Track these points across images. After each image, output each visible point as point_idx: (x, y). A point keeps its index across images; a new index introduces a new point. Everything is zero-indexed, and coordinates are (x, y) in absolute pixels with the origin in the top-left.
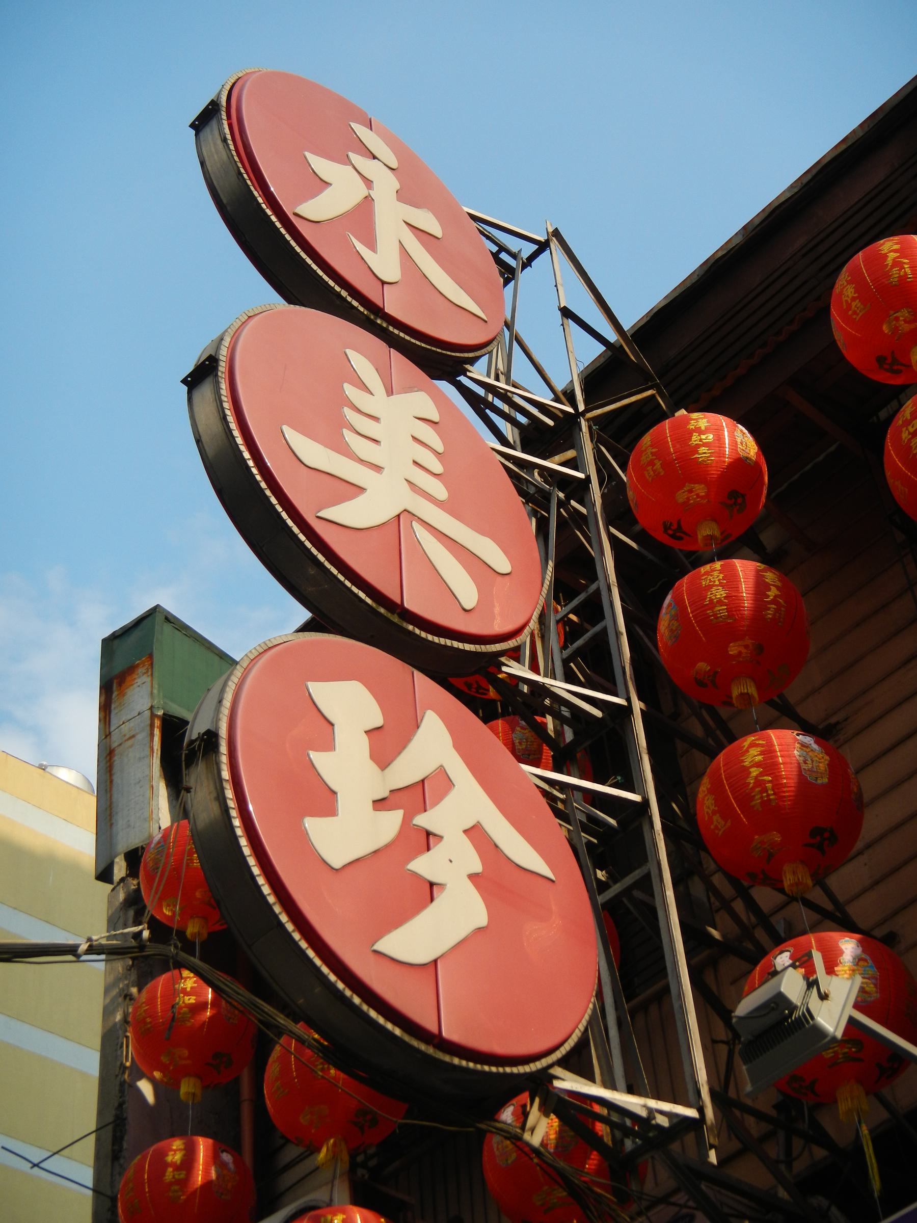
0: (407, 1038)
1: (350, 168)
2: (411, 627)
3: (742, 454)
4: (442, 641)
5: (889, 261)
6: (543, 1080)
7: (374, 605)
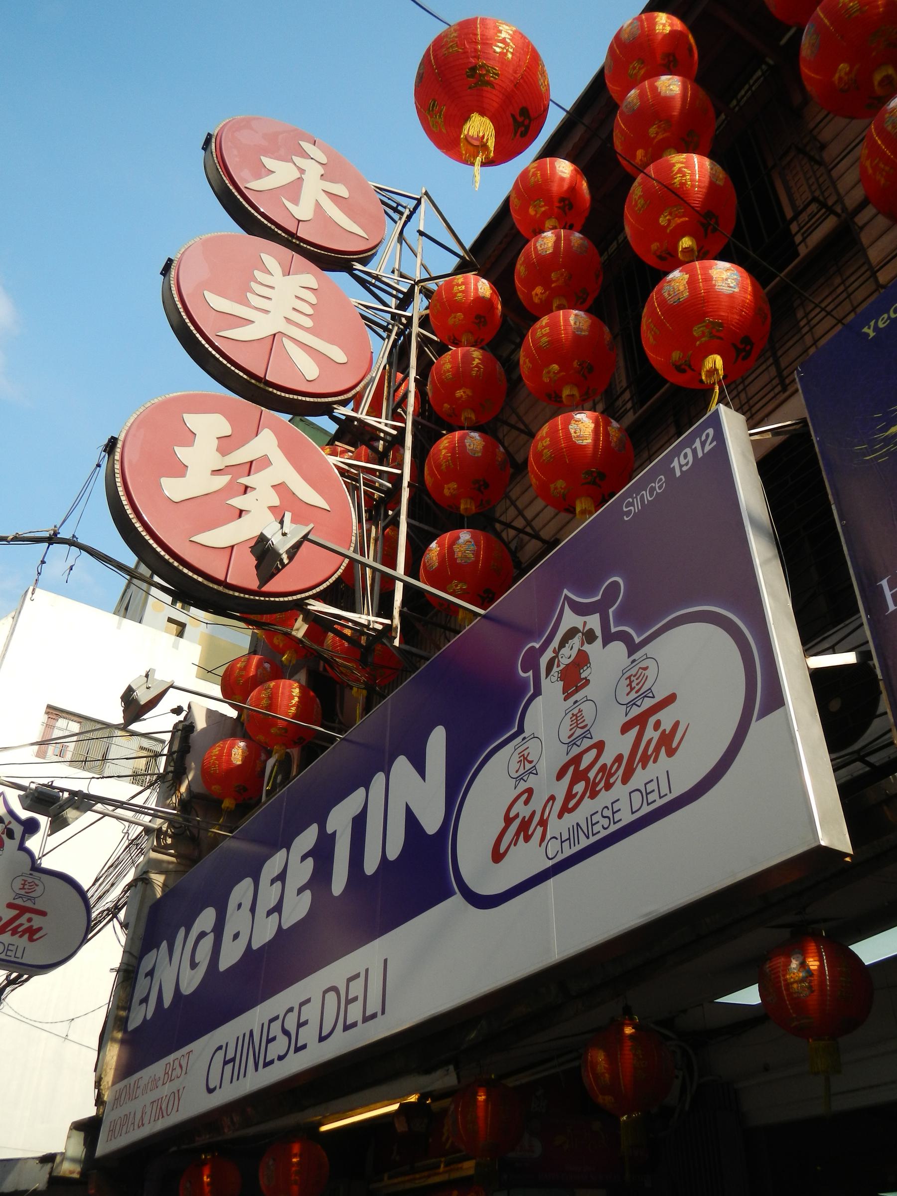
0: (206, 582)
1: (291, 165)
2: (271, 390)
3: (481, 295)
4: (291, 396)
5: (531, 174)
6: (300, 606)
7: (248, 379)
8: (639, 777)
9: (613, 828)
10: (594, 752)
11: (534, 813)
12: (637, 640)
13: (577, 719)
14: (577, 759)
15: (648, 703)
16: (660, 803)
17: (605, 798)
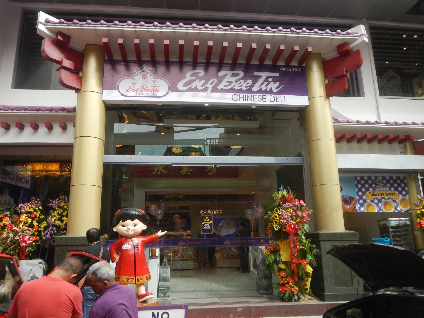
8: (153, 92)
9: (148, 96)
10: (146, 87)
11: (135, 89)
12: (155, 78)
13: (144, 82)
14: (144, 86)
15: (155, 85)
16: (155, 96)
17: (147, 92)
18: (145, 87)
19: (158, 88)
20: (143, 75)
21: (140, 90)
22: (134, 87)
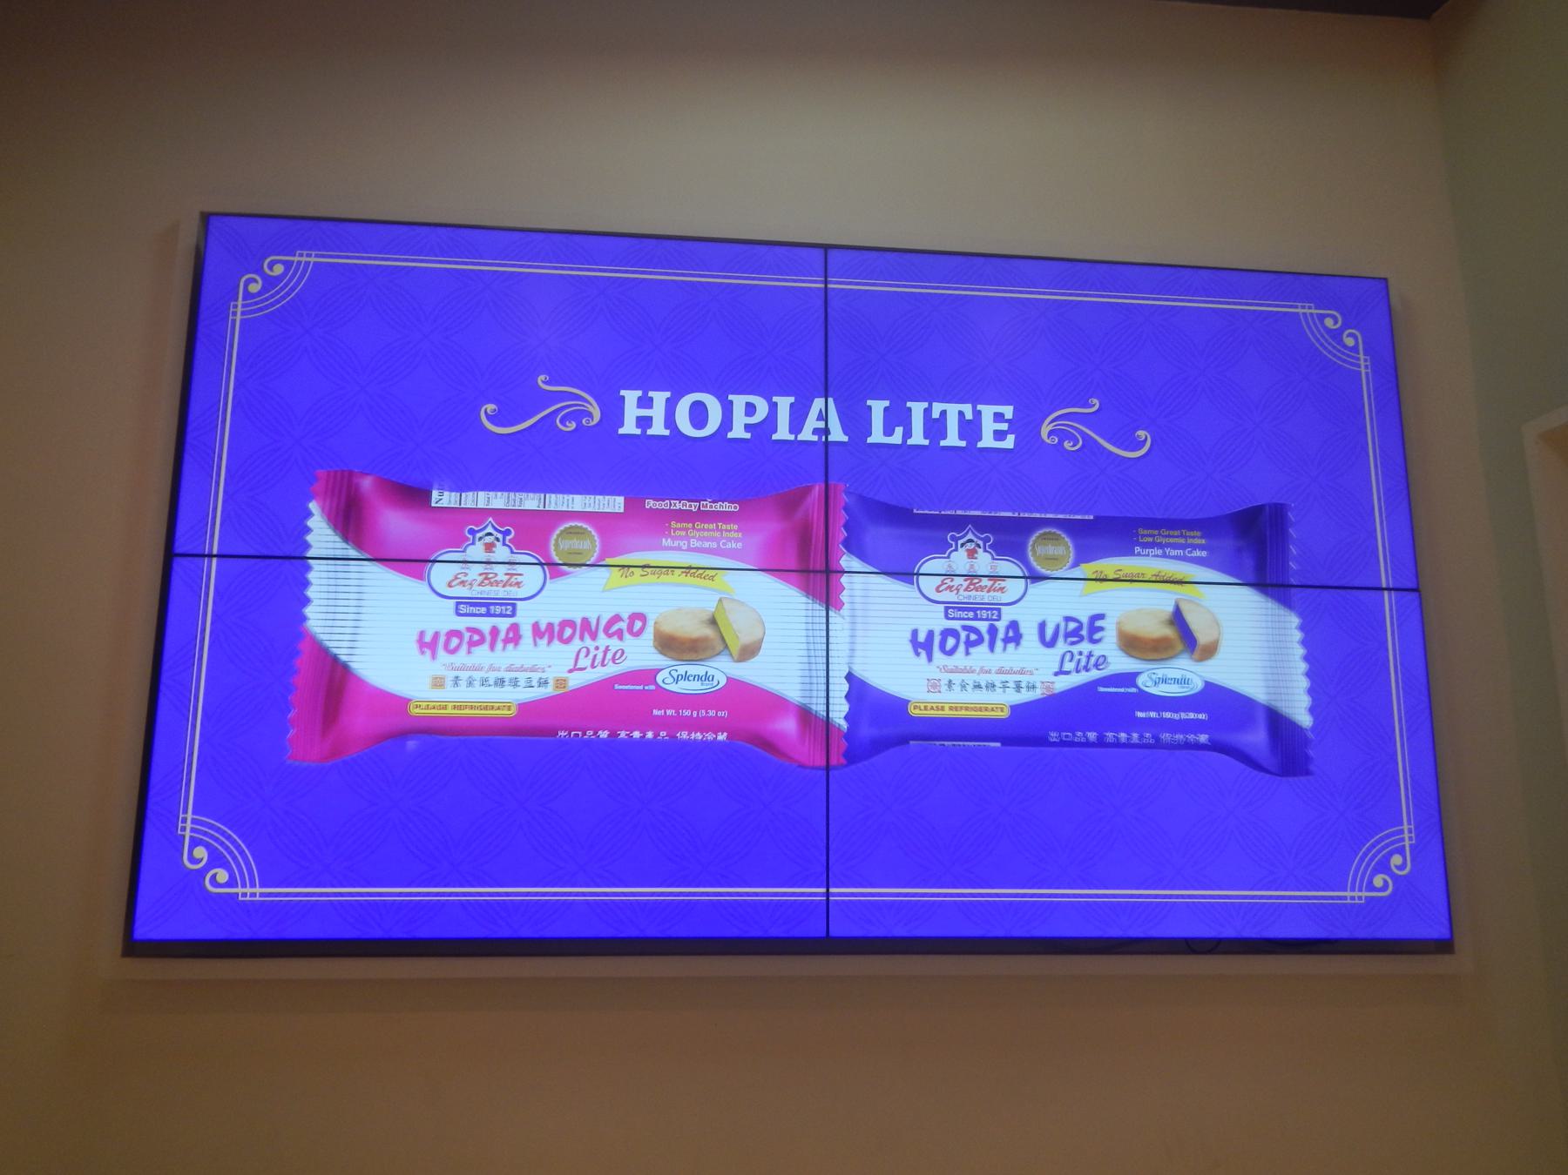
8: (508, 588)
15: (514, 572)
17: (495, 588)
18: (490, 576)
19: (520, 579)
20: (486, 544)
21: (478, 582)
22: (466, 574)
